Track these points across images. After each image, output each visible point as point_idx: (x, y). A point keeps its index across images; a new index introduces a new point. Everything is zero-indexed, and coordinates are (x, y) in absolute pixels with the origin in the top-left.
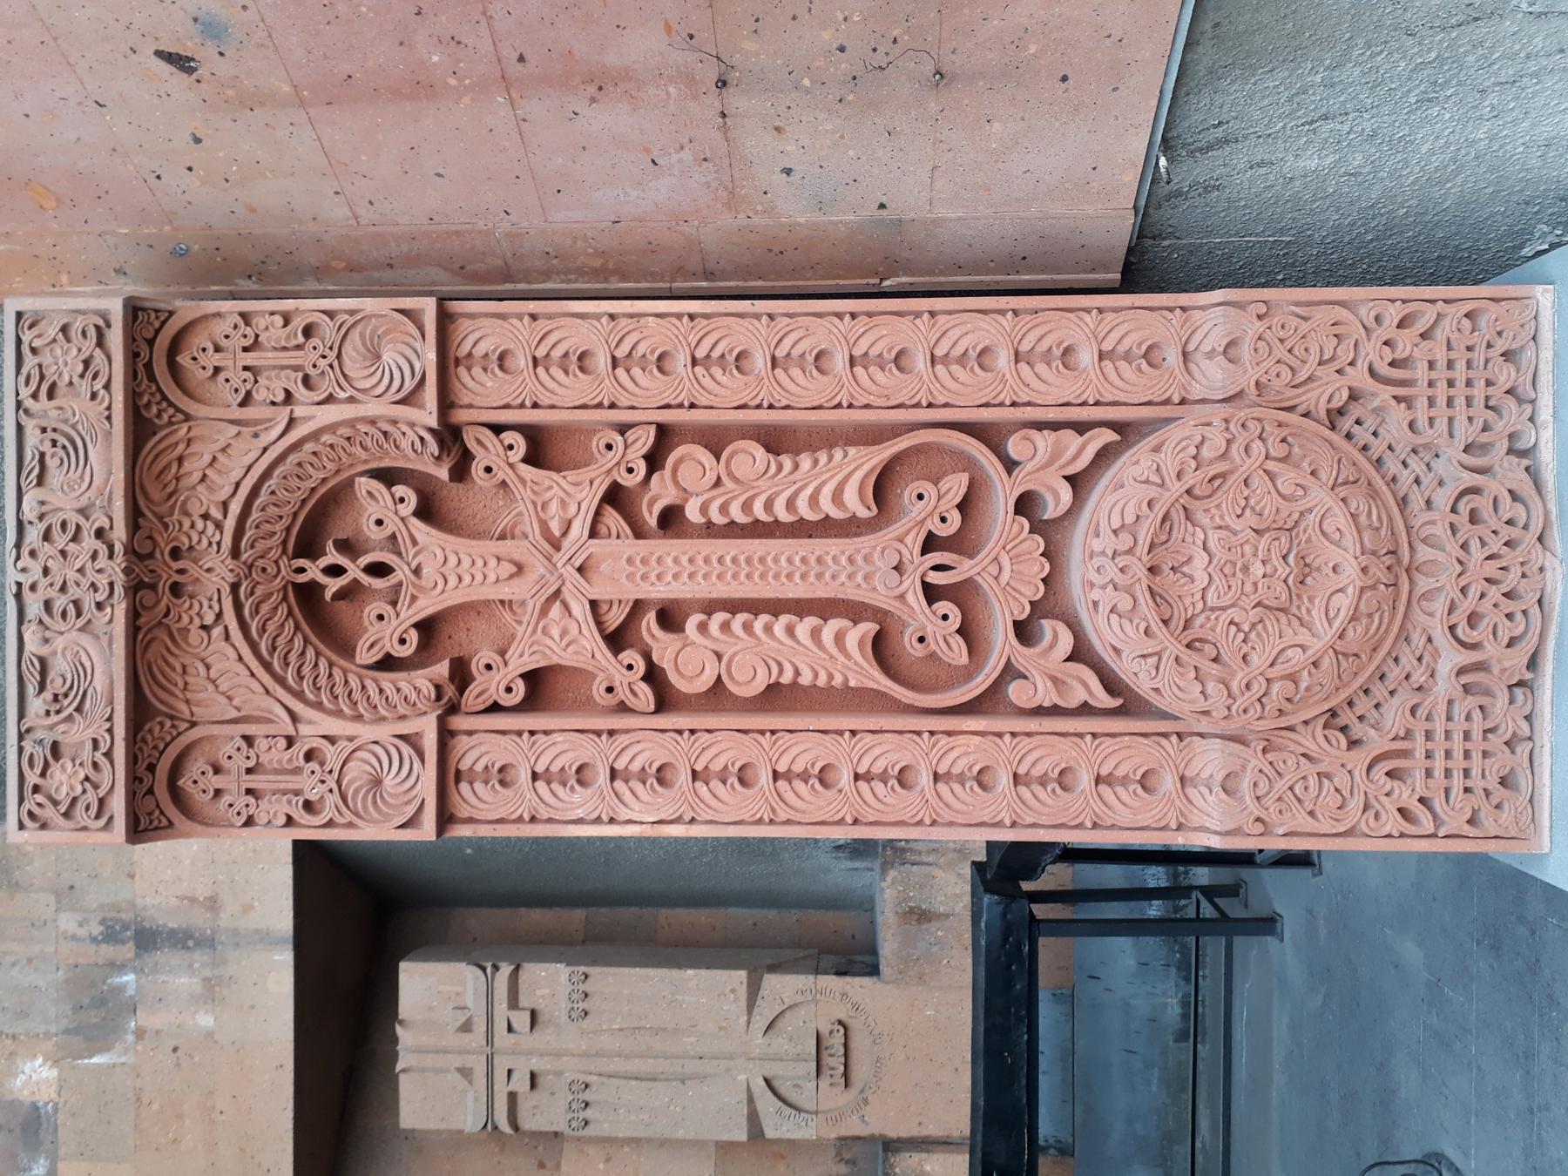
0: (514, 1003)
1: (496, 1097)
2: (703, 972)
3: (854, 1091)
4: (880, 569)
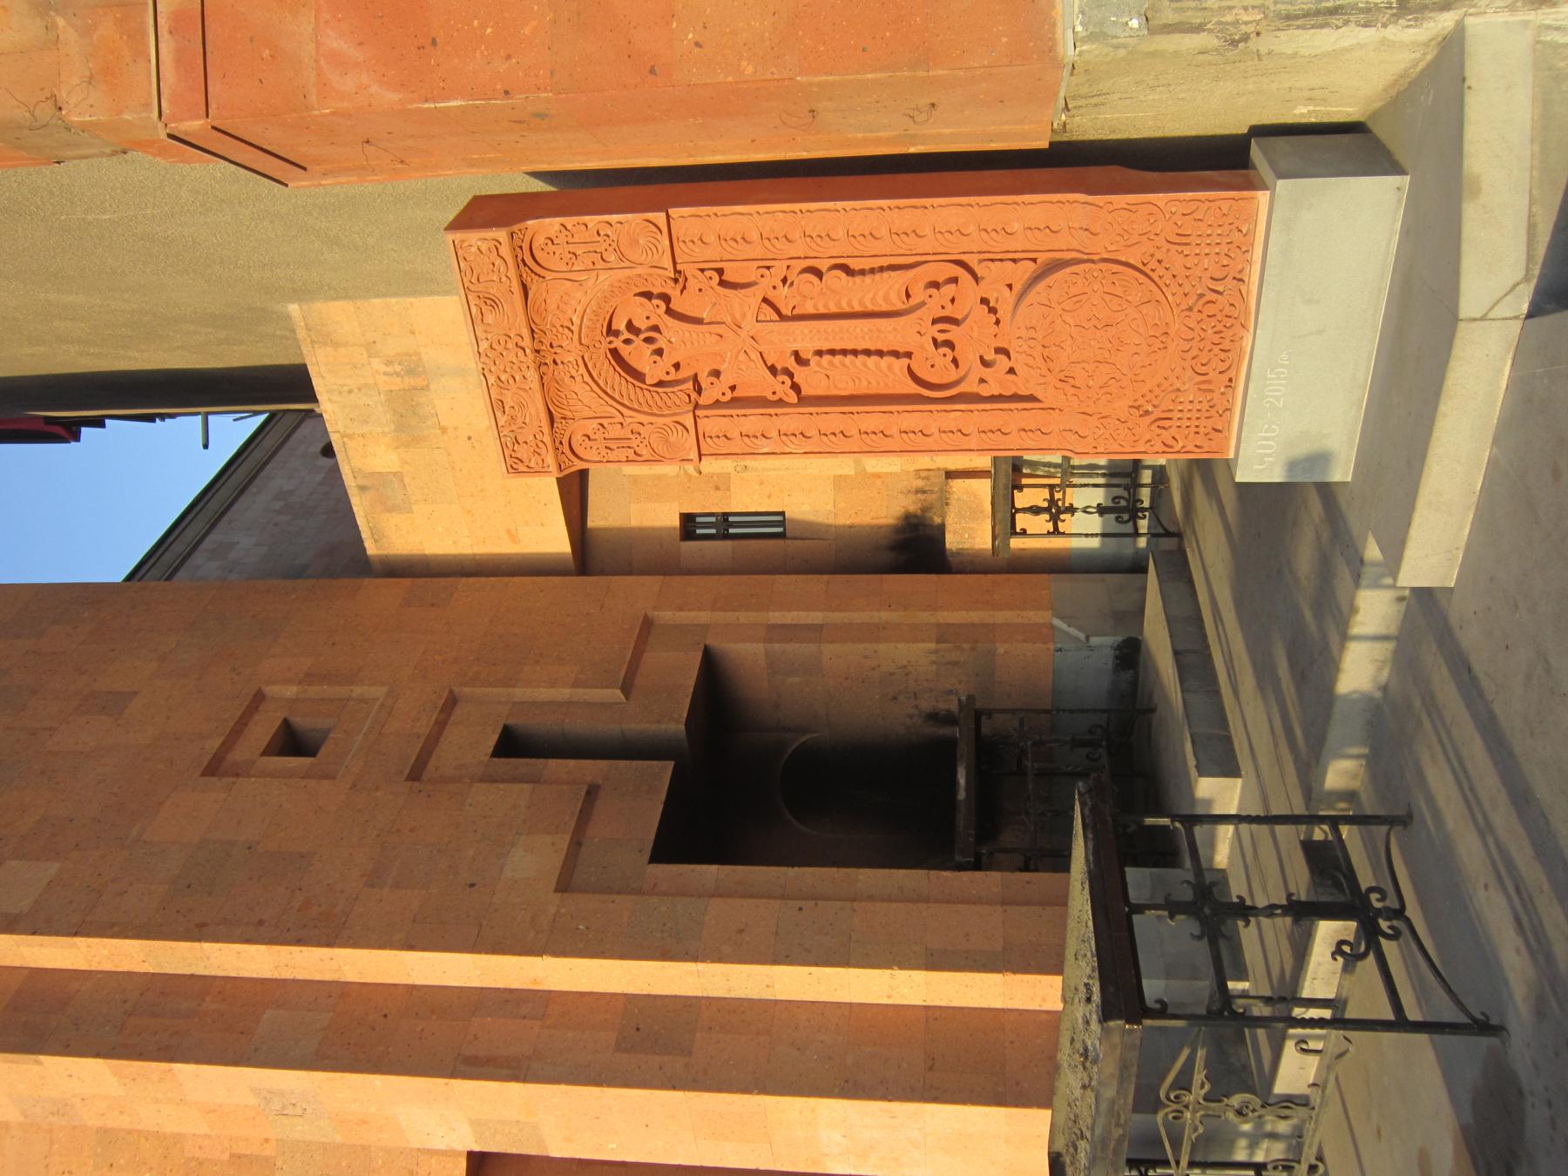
4: (908, 333)
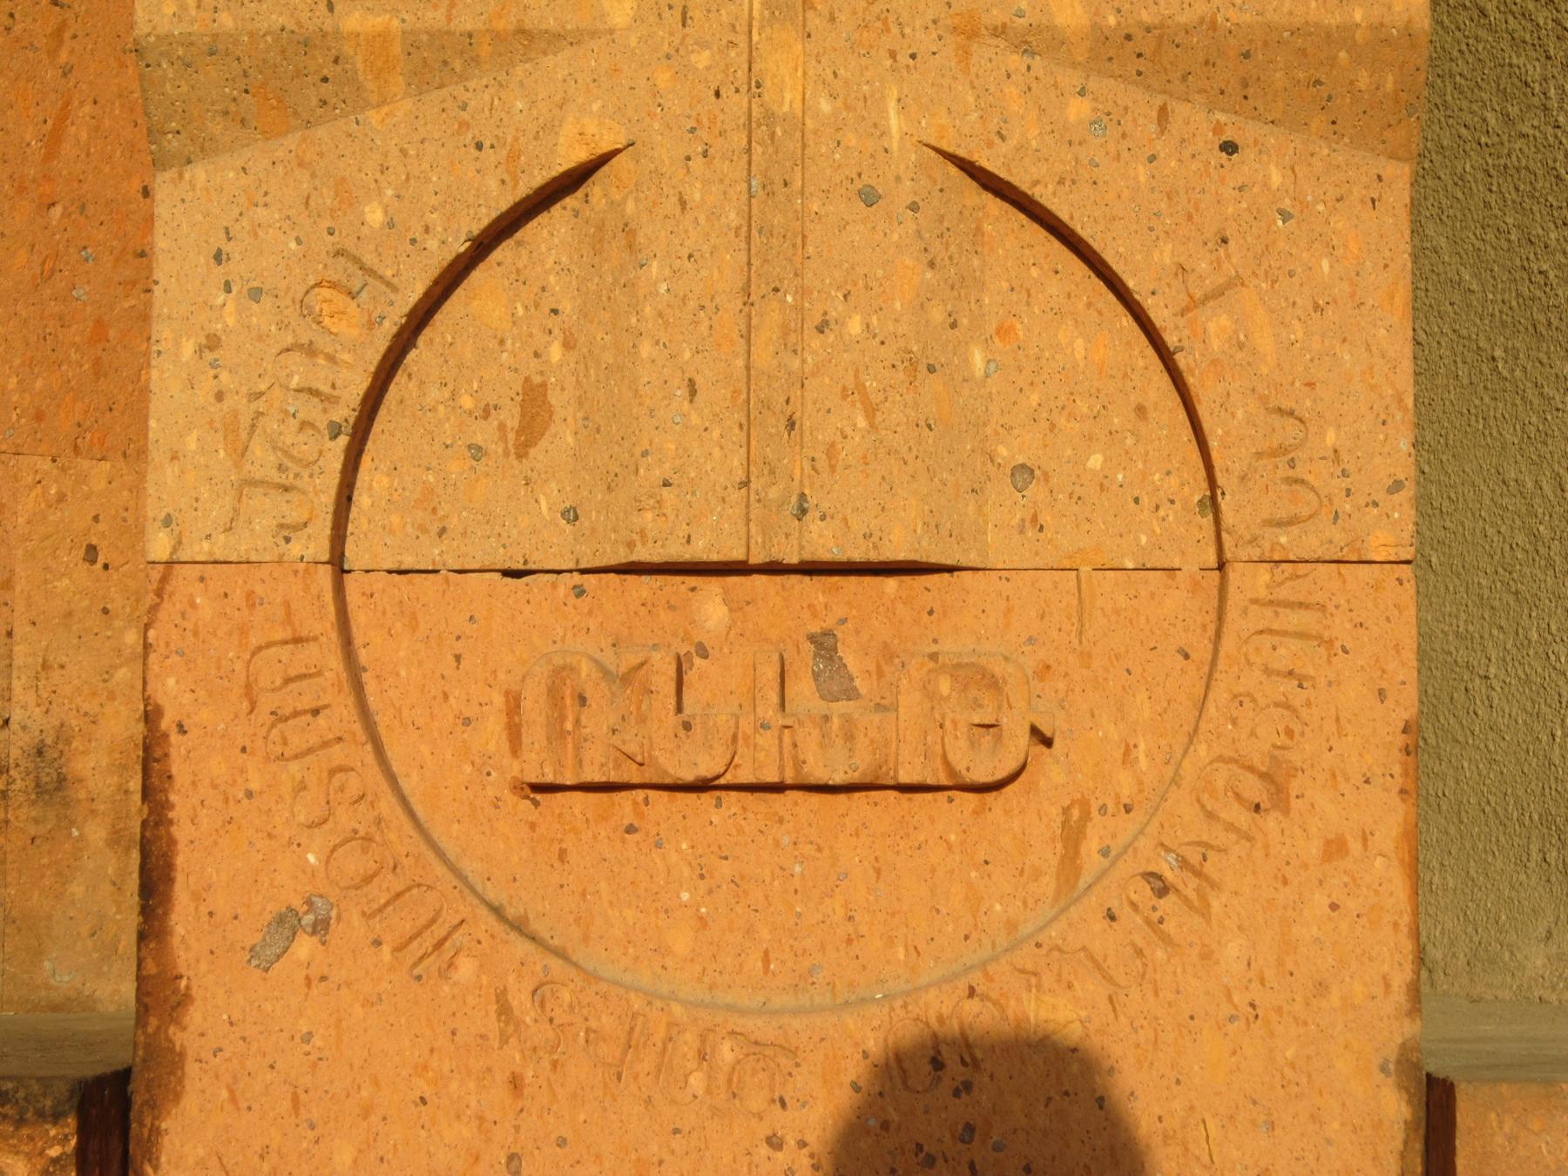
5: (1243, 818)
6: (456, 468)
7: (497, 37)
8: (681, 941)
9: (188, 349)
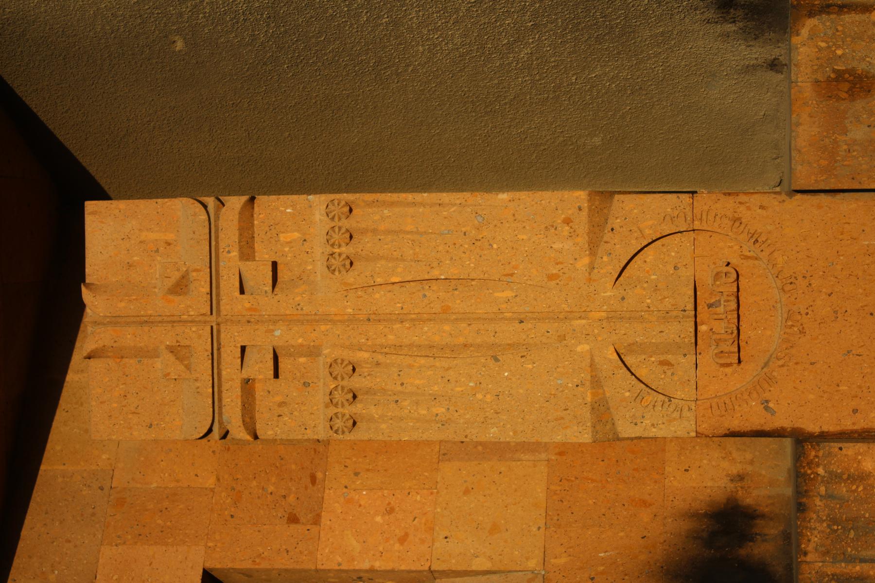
0: (247, 252)
1: (225, 386)
2: (523, 195)
3: (751, 370)
5: (743, 226)
6: (676, 378)
7: (592, 371)
8: (769, 333)
9: (654, 430)
